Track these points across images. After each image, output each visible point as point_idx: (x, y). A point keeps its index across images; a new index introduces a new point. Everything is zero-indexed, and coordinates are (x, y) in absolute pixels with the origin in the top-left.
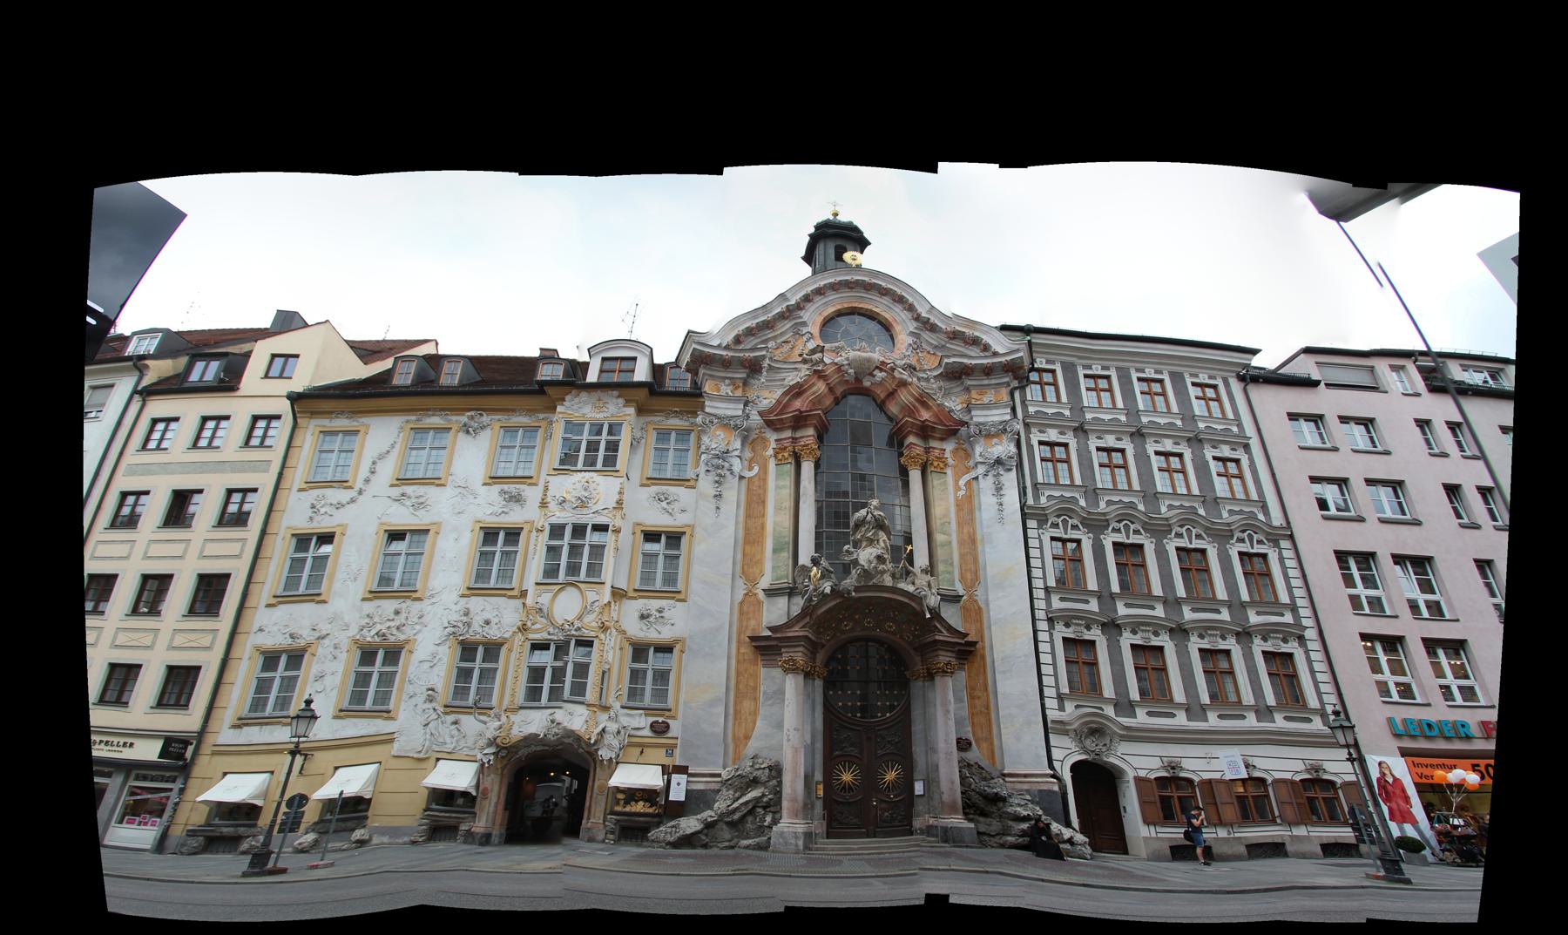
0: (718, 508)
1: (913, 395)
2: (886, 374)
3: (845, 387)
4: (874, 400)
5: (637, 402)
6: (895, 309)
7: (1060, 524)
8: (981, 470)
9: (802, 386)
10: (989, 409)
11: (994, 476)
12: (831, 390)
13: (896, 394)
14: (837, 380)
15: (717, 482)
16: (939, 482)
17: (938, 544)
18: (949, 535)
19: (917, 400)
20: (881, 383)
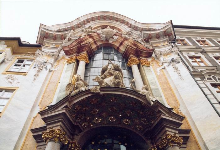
0: (35, 79)
1: (131, 43)
2: (118, 37)
3: (102, 43)
4: (114, 49)
5: (12, 47)
6: (122, 25)
7: (212, 78)
8: (165, 65)
9: (82, 39)
10: (162, 47)
11: (173, 66)
12: (95, 42)
13: (123, 43)
14: (97, 39)
15: (38, 71)
16: (147, 69)
17: (152, 89)
18: (157, 86)
19: (133, 44)
20: (116, 41)
